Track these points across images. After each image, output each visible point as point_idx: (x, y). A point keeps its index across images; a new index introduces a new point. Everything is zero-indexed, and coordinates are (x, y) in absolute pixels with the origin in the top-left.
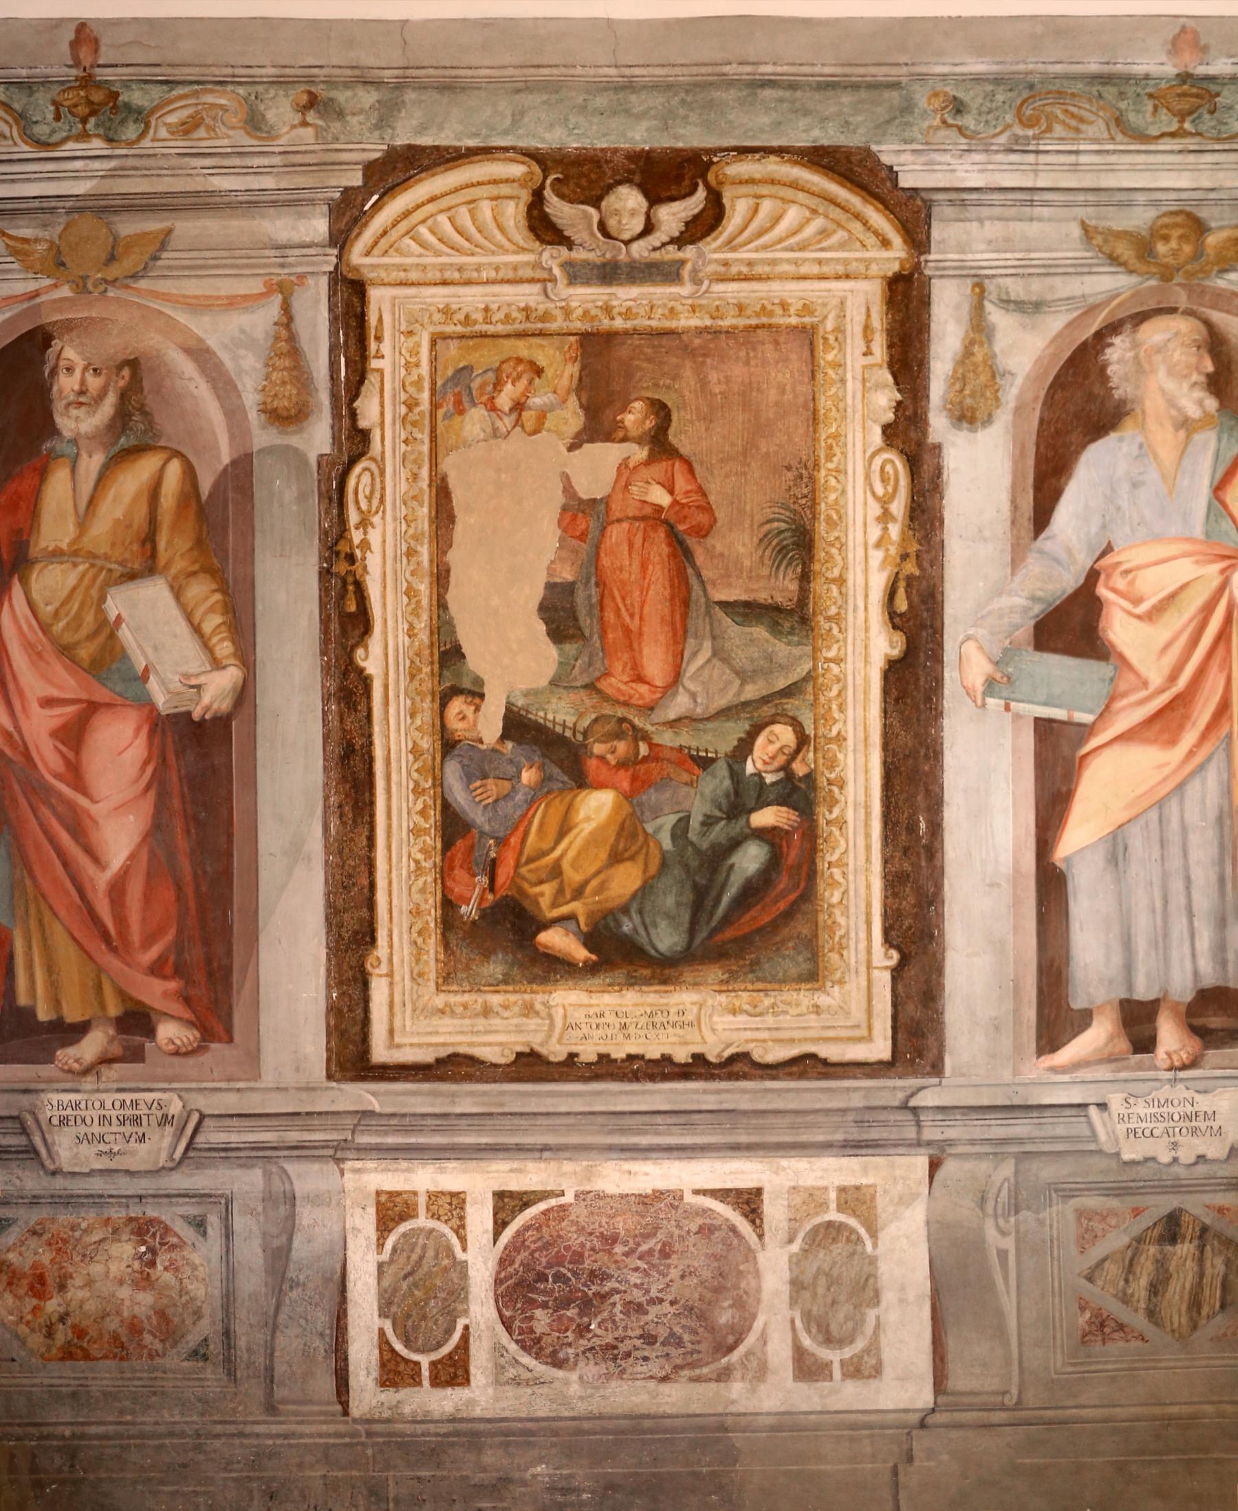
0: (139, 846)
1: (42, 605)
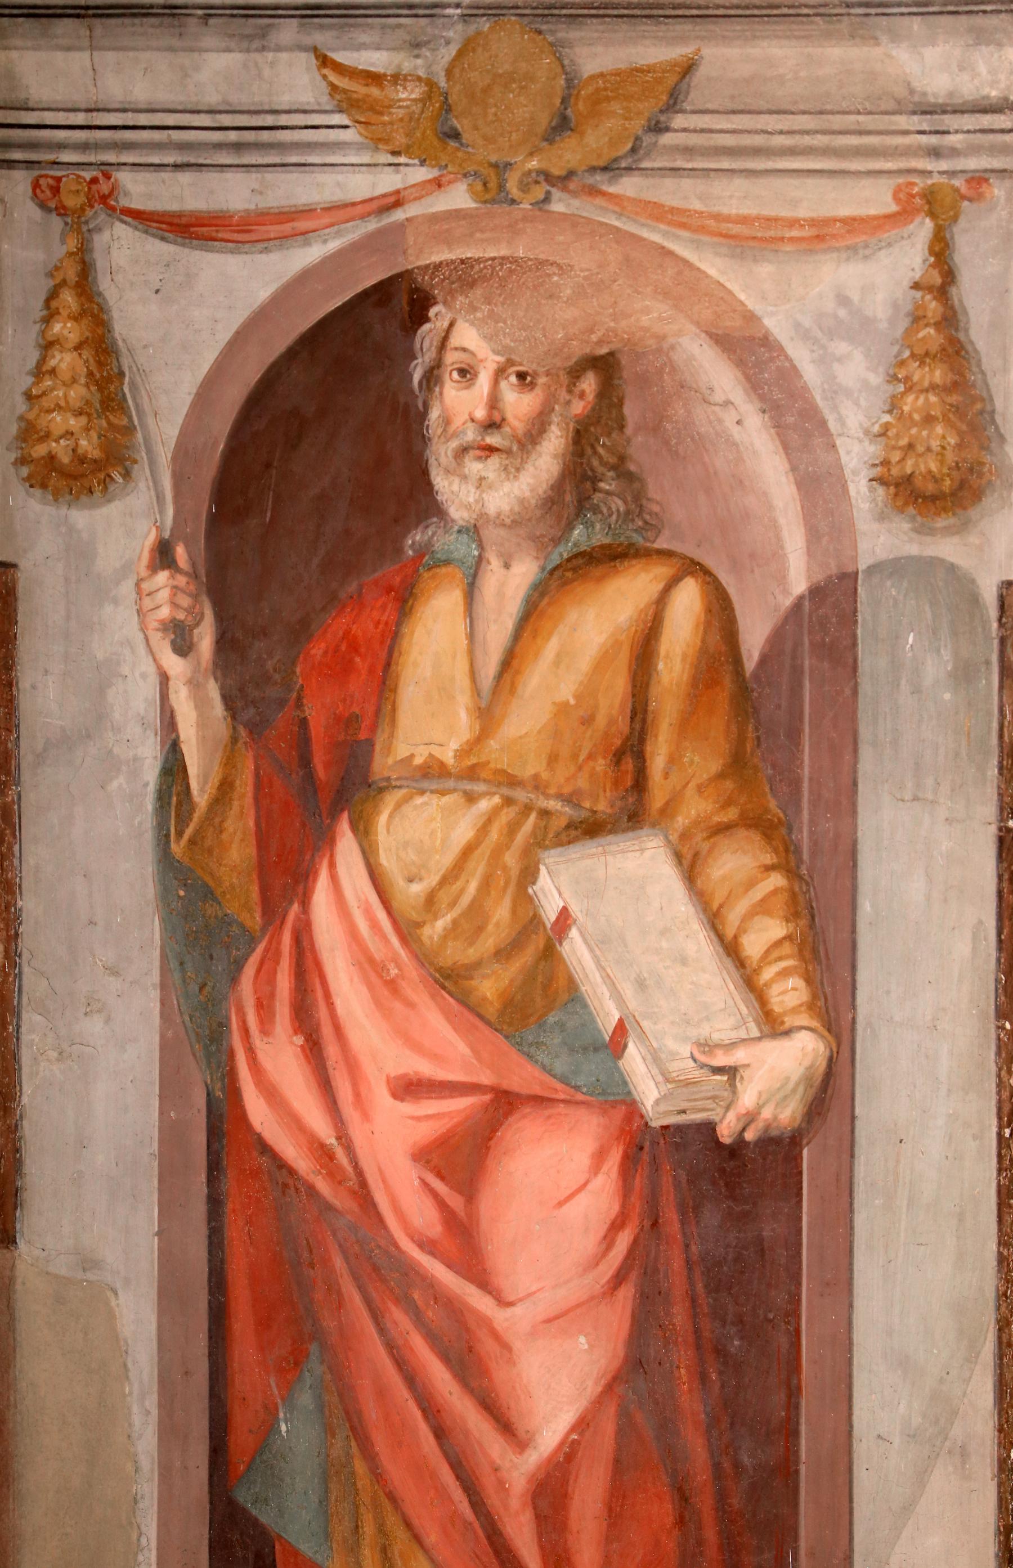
0: (598, 1403)
1: (401, 882)
